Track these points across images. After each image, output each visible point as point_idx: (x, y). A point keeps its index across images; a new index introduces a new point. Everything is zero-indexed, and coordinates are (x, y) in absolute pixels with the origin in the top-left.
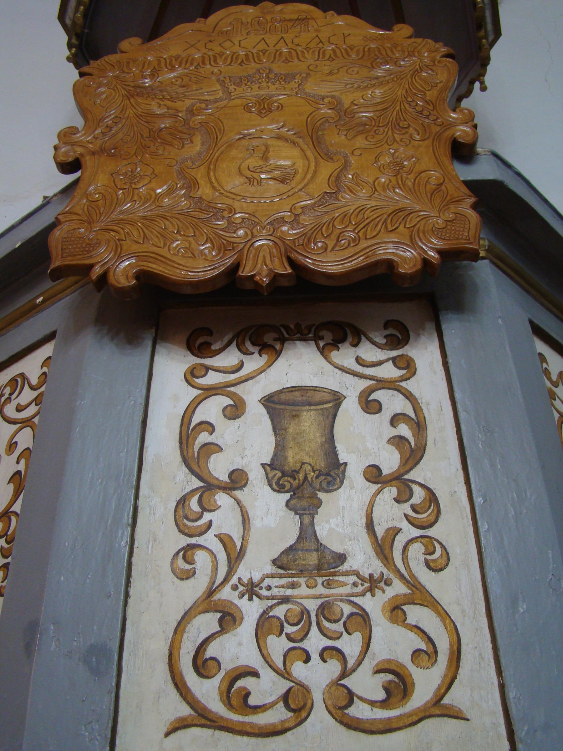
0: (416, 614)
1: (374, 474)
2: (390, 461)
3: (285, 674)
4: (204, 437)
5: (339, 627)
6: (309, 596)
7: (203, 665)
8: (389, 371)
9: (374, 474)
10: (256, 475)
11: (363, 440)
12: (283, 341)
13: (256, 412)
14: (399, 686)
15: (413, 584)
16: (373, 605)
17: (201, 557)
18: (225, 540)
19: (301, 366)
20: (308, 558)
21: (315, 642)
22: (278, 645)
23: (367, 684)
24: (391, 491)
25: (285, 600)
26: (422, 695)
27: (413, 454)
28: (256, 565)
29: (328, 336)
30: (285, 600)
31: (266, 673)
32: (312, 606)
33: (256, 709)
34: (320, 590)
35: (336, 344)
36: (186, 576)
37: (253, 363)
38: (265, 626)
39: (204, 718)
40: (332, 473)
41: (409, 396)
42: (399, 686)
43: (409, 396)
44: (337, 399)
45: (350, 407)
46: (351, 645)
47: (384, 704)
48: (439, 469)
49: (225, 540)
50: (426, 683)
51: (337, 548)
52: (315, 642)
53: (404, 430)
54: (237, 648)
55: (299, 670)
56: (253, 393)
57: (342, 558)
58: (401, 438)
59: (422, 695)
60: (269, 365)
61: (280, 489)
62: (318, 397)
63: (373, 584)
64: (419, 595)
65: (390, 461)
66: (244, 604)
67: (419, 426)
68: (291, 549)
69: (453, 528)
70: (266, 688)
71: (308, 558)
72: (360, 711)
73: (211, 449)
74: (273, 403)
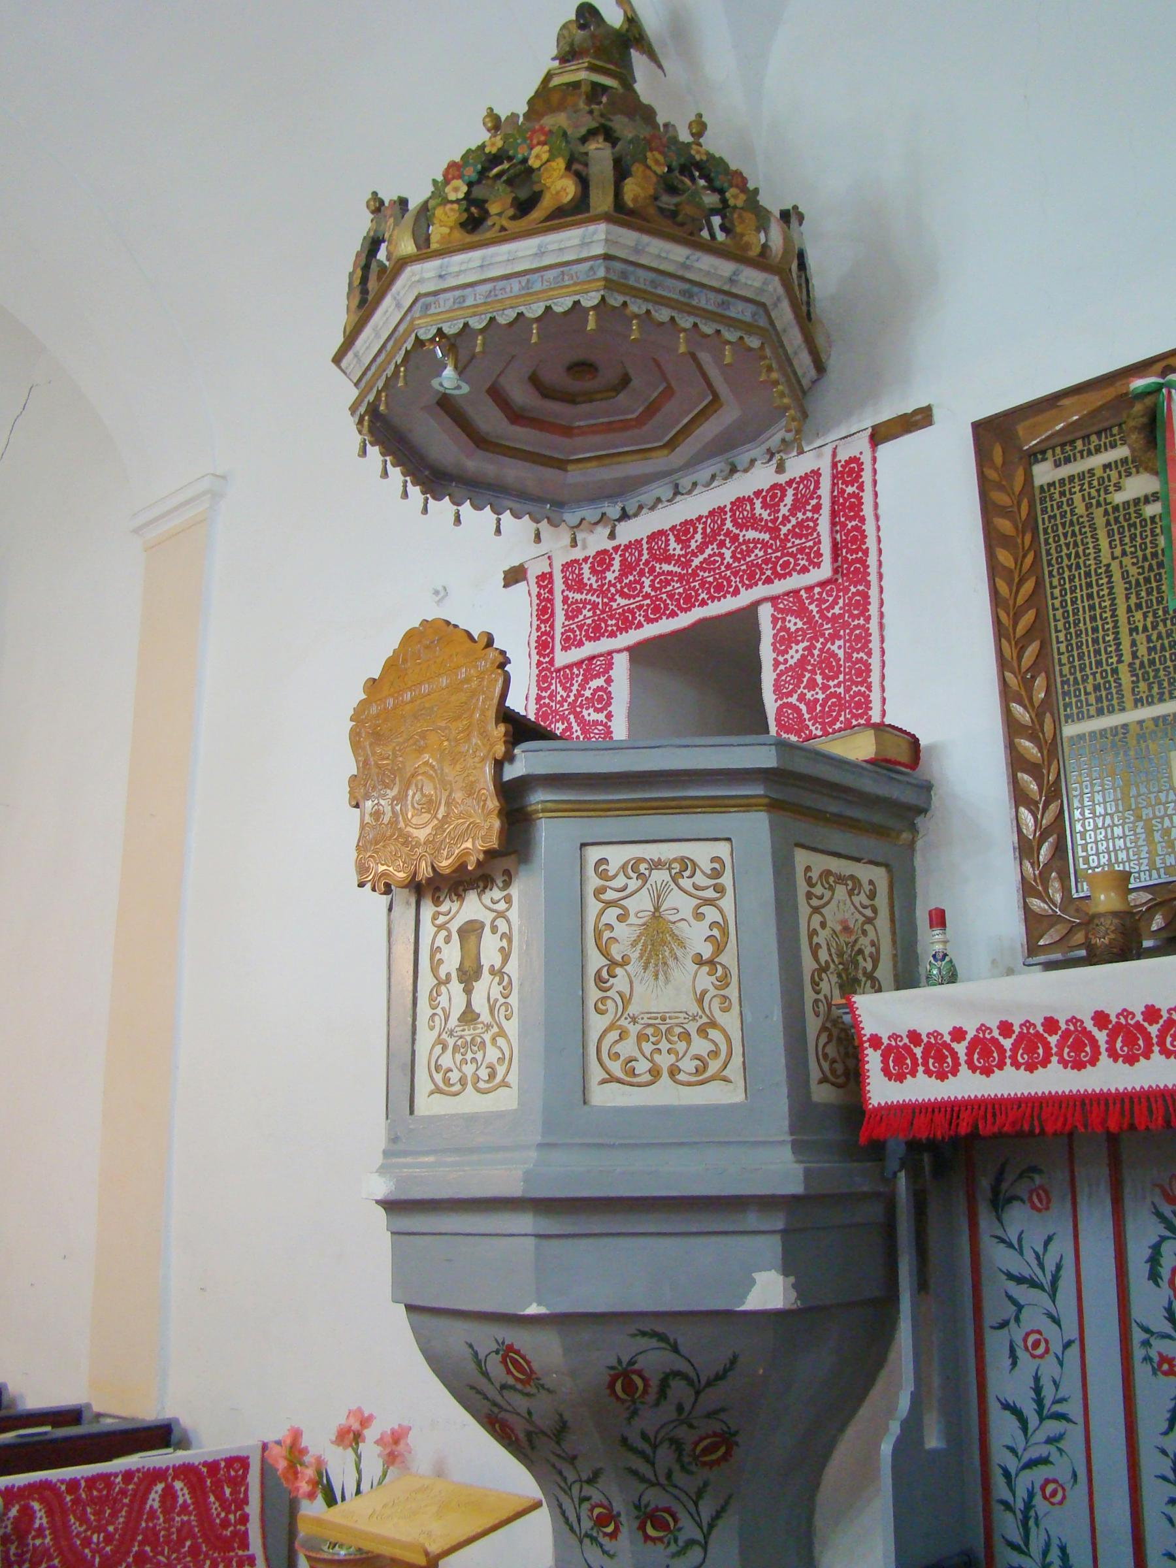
0: (501, 1041)
1: (492, 971)
2: (497, 962)
3: (460, 1070)
4: (438, 956)
5: (475, 1048)
6: (468, 1033)
7: (438, 1068)
8: (502, 906)
9: (492, 971)
10: (454, 975)
11: (490, 950)
12: (465, 890)
13: (455, 936)
14: (493, 1075)
15: (500, 1026)
16: (487, 1037)
17: (437, 1018)
18: (443, 1009)
19: (473, 907)
20: (469, 1016)
21: (469, 1056)
22: (459, 1057)
23: (484, 1073)
24: (497, 979)
25: (461, 1037)
26: (499, 1078)
27: (506, 955)
28: (453, 1022)
29: (481, 884)
30: (461, 1037)
31: (455, 1070)
32: (469, 1039)
33: (452, 1085)
34: (472, 1032)
35: (483, 891)
36: (432, 1028)
37: (455, 906)
38: (456, 1048)
39: (438, 1090)
40: (477, 973)
41: (508, 921)
42: (493, 1075)
43: (508, 921)
44: (482, 926)
45: (487, 929)
46: (479, 1056)
47: (487, 1082)
48: (512, 968)
49: (443, 1009)
50: (501, 1070)
51: (477, 1011)
52: (469, 1056)
53: (505, 943)
54: (446, 1061)
55: (464, 1068)
56: (454, 926)
57: (479, 1015)
58: (503, 948)
59: (499, 1078)
60: (461, 905)
61: (461, 982)
62: (477, 926)
63: (488, 1027)
64: (502, 1033)
65: (497, 962)
66: (449, 1039)
67: (510, 941)
68: (464, 1013)
69: (513, 1000)
70: (454, 1076)
71: (469, 1016)
72: (481, 1085)
73: (441, 961)
74: (462, 932)
